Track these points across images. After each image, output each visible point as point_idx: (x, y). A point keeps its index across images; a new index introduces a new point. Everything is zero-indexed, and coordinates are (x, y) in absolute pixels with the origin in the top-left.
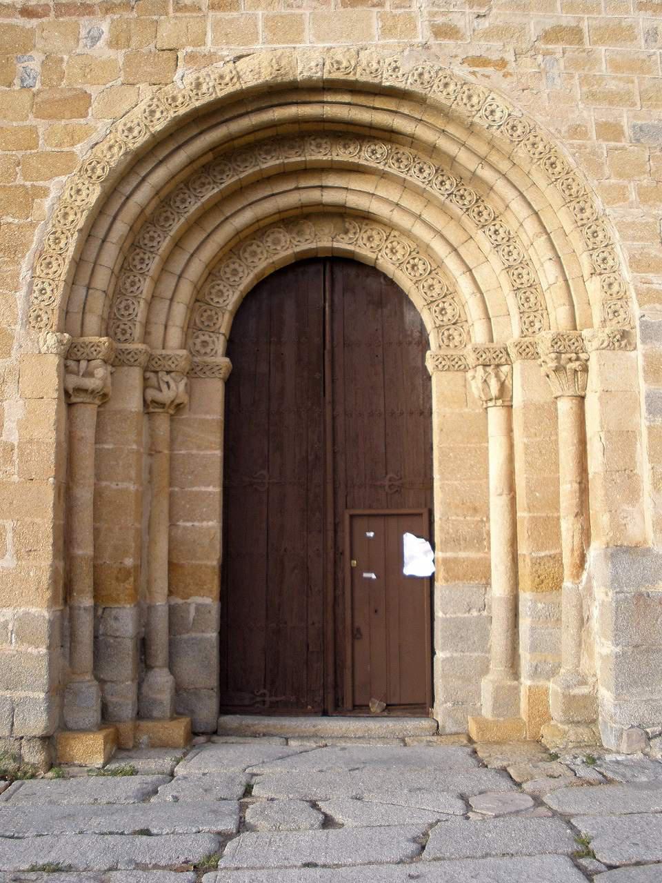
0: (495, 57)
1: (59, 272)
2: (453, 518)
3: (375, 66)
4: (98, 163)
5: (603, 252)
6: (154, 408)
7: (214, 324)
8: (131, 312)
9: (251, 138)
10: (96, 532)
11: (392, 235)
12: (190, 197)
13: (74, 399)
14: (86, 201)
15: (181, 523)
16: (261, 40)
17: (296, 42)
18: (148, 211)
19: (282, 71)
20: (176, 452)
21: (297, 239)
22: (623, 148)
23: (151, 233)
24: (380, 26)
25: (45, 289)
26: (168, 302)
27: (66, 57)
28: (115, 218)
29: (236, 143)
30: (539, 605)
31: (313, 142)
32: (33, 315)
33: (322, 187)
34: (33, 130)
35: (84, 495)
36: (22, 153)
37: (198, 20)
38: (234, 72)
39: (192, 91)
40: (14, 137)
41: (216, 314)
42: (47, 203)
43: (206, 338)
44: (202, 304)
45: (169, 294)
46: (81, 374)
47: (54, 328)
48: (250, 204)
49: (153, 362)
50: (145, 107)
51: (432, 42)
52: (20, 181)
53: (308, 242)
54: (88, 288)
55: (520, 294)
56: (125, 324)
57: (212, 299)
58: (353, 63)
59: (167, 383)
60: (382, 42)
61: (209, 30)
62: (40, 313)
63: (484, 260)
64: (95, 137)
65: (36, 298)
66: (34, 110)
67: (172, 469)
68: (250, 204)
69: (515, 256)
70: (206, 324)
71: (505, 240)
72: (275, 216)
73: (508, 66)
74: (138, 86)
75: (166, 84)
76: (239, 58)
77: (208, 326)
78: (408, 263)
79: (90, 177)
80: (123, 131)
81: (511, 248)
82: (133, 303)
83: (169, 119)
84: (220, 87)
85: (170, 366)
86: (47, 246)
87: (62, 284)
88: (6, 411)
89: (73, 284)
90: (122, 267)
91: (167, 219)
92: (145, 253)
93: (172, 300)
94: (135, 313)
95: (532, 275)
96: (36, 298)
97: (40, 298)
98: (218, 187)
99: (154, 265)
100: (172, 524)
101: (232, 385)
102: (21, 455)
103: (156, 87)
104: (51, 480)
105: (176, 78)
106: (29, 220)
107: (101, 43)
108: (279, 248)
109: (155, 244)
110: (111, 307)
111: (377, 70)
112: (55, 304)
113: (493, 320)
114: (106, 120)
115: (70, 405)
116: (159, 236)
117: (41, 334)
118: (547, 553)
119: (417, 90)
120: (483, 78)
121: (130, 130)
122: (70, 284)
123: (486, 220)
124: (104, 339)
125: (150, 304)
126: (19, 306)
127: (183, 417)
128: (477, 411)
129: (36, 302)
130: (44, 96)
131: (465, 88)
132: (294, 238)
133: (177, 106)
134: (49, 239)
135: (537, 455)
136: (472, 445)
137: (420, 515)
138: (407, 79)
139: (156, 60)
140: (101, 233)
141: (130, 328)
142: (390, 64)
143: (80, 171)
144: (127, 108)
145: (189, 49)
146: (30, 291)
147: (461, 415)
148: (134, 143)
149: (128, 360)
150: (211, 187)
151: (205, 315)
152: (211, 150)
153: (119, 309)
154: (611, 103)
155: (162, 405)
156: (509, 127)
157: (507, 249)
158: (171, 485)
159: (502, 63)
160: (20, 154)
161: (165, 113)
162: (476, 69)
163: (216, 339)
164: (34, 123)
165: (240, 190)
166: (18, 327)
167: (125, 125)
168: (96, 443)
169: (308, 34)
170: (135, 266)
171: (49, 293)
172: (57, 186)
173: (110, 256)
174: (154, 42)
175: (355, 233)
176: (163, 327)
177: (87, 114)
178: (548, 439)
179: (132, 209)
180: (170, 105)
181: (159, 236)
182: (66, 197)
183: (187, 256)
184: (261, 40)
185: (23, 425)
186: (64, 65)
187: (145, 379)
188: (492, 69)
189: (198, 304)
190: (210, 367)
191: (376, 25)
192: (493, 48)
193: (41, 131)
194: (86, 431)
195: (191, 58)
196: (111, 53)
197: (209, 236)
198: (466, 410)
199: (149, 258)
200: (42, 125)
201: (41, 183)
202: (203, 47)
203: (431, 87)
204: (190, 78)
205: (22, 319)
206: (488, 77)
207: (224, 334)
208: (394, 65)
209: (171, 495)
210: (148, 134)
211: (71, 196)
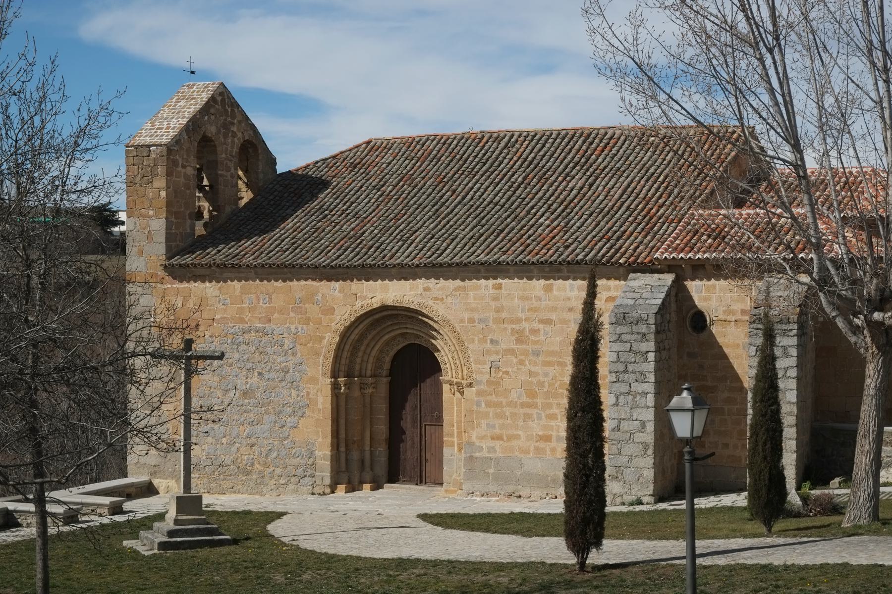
10: (346, 430)
34: (321, 318)
35: (342, 422)
67: (371, 410)
115: (337, 397)
172: (328, 335)
179: (350, 341)
182: (330, 339)
191: (408, 287)
192: (439, 294)
194: (342, 403)
195: (360, 297)
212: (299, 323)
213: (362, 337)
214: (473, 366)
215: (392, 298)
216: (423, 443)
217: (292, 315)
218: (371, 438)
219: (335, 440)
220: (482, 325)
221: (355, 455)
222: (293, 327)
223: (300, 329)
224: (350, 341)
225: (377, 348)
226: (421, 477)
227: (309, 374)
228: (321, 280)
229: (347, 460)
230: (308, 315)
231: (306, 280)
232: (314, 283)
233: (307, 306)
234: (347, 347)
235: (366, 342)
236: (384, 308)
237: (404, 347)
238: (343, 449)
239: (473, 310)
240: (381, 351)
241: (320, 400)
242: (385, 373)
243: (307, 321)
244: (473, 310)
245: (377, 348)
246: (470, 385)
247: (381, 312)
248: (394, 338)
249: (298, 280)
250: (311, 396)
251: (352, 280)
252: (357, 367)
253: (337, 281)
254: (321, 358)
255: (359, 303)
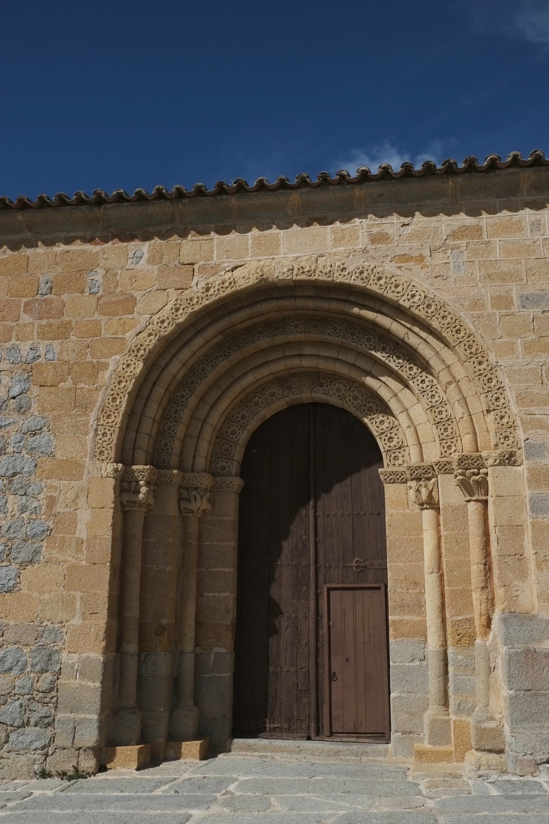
0: (415, 254)
1: (116, 422)
2: (399, 590)
3: (329, 269)
4: (142, 345)
5: (496, 393)
6: (186, 513)
7: (230, 453)
8: (168, 447)
9: (248, 323)
10: (142, 600)
11: (353, 386)
12: (208, 366)
13: (126, 509)
14: (133, 372)
15: (206, 594)
16: (250, 254)
17: (274, 255)
18: (179, 377)
19: (265, 277)
20: (203, 544)
21: (287, 392)
22: (513, 314)
23: (182, 392)
24: (333, 239)
25: (106, 434)
26: (196, 439)
27: (119, 272)
28: (155, 383)
29: (238, 327)
30: (460, 657)
31: (292, 324)
32: (98, 451)
33: (301, 356)
34: (98, 323)
35: (135, 575)
36: (91, 339)
37: (208, 241)
38: (232, 279)
39: (203, 293)
40: (84, 329)
41: (231, 446)
42: (107, 374)
43: (224, 464)
44: (221, 440)
45: (196, 434)
46: (132, 491)
47: (112, 460)
48: (251, 370)
49: (185, 482)
50: (172, 306)
51: (369, 247)
52: (89, 358)
53: (295, 393)
54: (137, 432)
55: (440, 426)
56: (164, 456)
57: (228, 436)
58: (313, 268)
59: (195, 496)
60: (334, 250)
61: (215, 248)
62: (103, 449)
63: (416, 401)
64: (138, 328)
65: (100, 439)
66: (98, 310)
68: (251, 370)
69: (436, 398)
70: (224, 453)
71: (429, 388)
72: (270, 377)
73: (425, 261)
74: (168, 290)
75: (187, 289)
76: (236, 268)
77: (225, 455)
78: (365, 406)
79: (136, 356)
80: (158, 323)
81: (434, 392)
82: (170, 441)
83: (188, 314)
84: (222, 290)
85: (197, 484)
86: (107, 404)
87: (117, 430)
88: (79, 517)
89: (126, 429)
90: (162, 416)
91: (192, 382)
92: (177, 407)
93: (198, 438)
94: (171, 448)
95: (449, 412)
96: (100, 439)
97: (103, 440)
98: (227, 359)
99: (185, 415)
100: (199, 595)
101: (244, 496)
102: (88, 547)
103: (180, 291)
104: (108, 564)
105: (193, 283)
106: (95, 386)
107: (143, 261)
108: (274, 398)
109: (184, 400)
110: (155, 444)
111: (330, 271)
112: (112, 443)
113: (423, 445)
114: (146, 316)
115: (125, 513)
116: (187, 394)
117: (103, 464)
118: (464, 617)
119: (358, 284)
120: (406, 271)
121: (163, 322)
122: (124, 430)
123: (415, 373)
124: (148, 467)
125: (183, 442)
126: (89, 445)
127: (208, 518)
128: (416, 511)
129: (100, 442)
130: (104, 299)
131: (393, 280)
132: (285, 391)
133: (193, 305)
134: (109, 399)
135: (454, 544)
136: (412, 537)
137: (379, 588)
138: (351, 277)
139: (180, 272)
140: (145, 393)
141: (168, 458)
142: (339, 267)
143: (129, 352)
144: (160, 307)
145: (202, 263)
146: (96, 435)
147: (404, 515)
148: (165, 331)
149: (167, 481)
150: (222, 359)
151: (224, 447)
152: (220, 333)
153: (160, 446)
154: (503, 280)
155: (192, 512)
156: (425, 306)
157: (430, 394)
158: (199, 566)
159: (421, 258)
160: (89, 340)
161: (185, 310)
162: (402, 265)
163: (231, 464)
164: (98, 318)
165: (244, 360)
166: (87, 459)
167: (159, 318)
168: (143, 538)
169: (282, 249)
170: (171, 416)
171: (109, 436)
172: (114, 362)
173: (153, 410)
174: (178, 259)
175: (327, 386)
176: (192, 458)
177: (134, 311)
178: (462, 532)
180: (189, 304)
181: (187, 394)
182: (120, 369)
183: (208, 407)
184: (250, 254)
185: (89, 526)
186: (118, 277)
187: (180, 494)
188: (413, 263)
189: (219, 440)
190: (226, 484)
192: (414, 247)
193: (103, 324)
195: (203, 269)
196: (150, 267)
197: (223, 393)
198: (408, 511)
199: (180, 410)
200: (104, 319)
201: (103, 360)
202: (211, 262)
203: (369, 281)
204: (202, 284)
205: (90, 454)
206: (410, 270)
207: (236, 461)
208: (342, 266)
209: (199, 574)
210: (174, 325)
211: (123, 369)
212: (43, 335)
213: (193, 374)
214: (514, 408)
215: (288, 264)
216: (324, 632)
217: (25, 318)
218: (199, 624)
219: (115, 623)
220: (532, 312)
221: (161, 665)
222: (25, 347)
223: (42, 351)
224: (167, 377)
225: (223, 405)
226: (318, 718)
227: (59, 455)
228: (105, 240)
229: (139, 677)
230: (66, 318)
231: (68, 241)
232: (88, 247)
233: (65, 297)
234: (159, 391)
235: (200, 389)
236: (266, 291)
237: (275, 416)
238: (132, 648)
239: (504, 277)
240: (228, 419)
241: (84, 516)
242: (235, 468)
243: (63, 332)
244: (504, 277)
245: (223, 405)
246: (509, 460)
247: (252, 304)
248: (260, 388)
249: (50, 243)
250: (59, 508)
251: (184, 235)
252: (176, 447)
253: (146, 238)
254: (93, 416)
255: (197, 285)
